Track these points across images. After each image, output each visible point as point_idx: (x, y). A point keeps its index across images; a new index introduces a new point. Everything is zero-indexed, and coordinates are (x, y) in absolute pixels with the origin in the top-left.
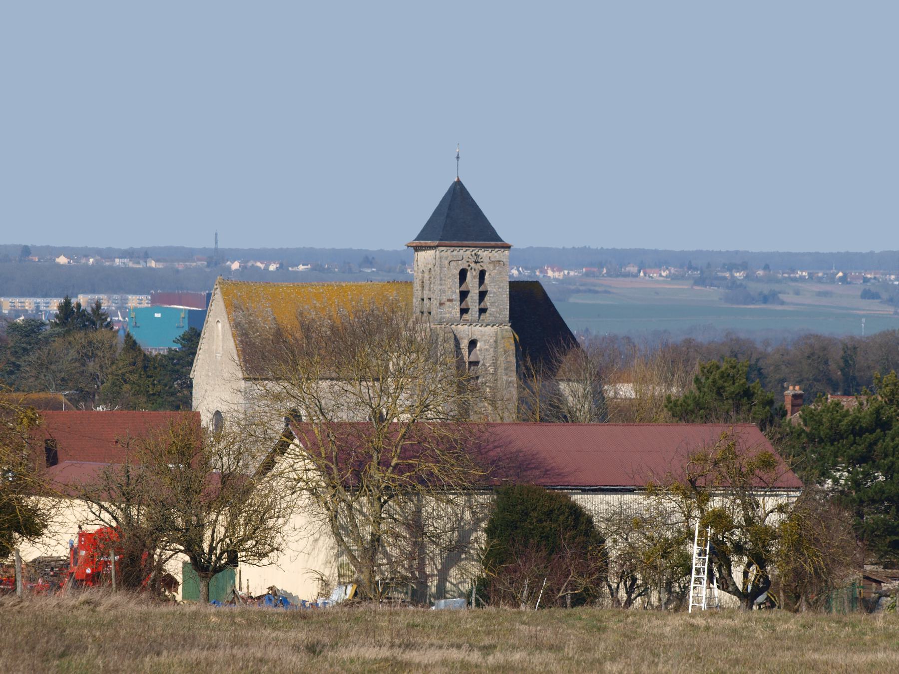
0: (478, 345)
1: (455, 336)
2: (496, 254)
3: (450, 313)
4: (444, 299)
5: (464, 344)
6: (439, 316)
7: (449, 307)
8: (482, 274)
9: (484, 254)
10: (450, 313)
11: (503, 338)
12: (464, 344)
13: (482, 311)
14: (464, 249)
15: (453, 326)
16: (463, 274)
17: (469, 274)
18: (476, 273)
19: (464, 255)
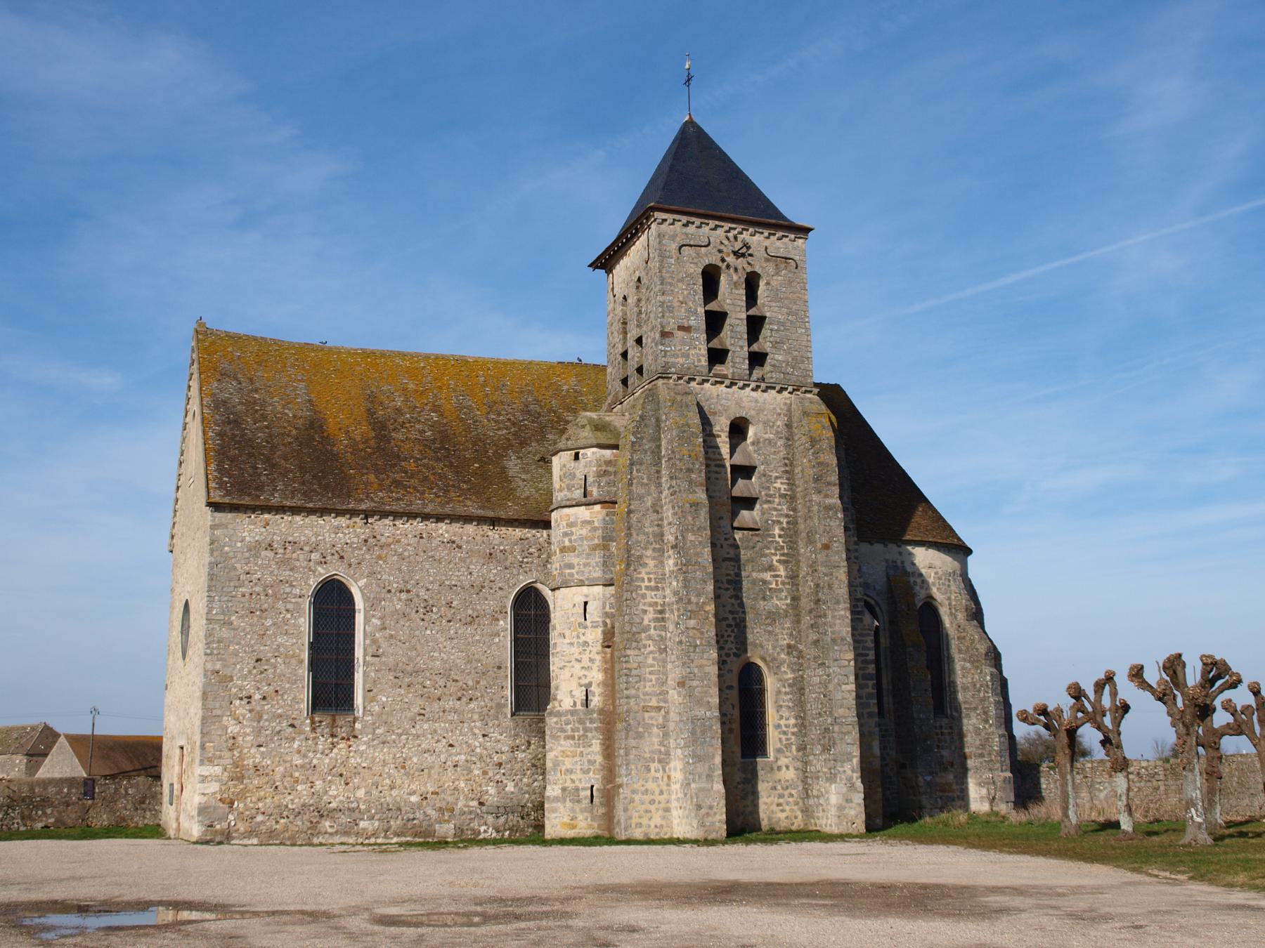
0: (751, 432)
1: (698, 405)
2: (779, 243)
3: (687, 356)
4: (671, 325)
5: (721, 427)
6: (661, 361)
7: (683, 342)
8: (752, 283)
9: (758, 240)
10: (687, 356)
11: (805, 413)
12: (721, 427)
13: (757, 359)
14: (712, 223)
15: (693, 384)
16: (710, 279)
17: (723, 278)
18: (739, 278)
19: (715, 238)
